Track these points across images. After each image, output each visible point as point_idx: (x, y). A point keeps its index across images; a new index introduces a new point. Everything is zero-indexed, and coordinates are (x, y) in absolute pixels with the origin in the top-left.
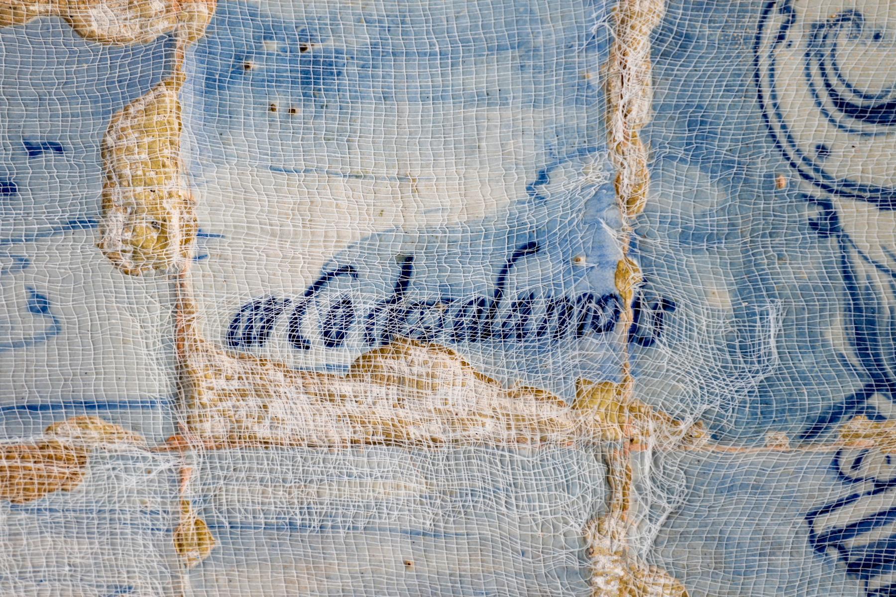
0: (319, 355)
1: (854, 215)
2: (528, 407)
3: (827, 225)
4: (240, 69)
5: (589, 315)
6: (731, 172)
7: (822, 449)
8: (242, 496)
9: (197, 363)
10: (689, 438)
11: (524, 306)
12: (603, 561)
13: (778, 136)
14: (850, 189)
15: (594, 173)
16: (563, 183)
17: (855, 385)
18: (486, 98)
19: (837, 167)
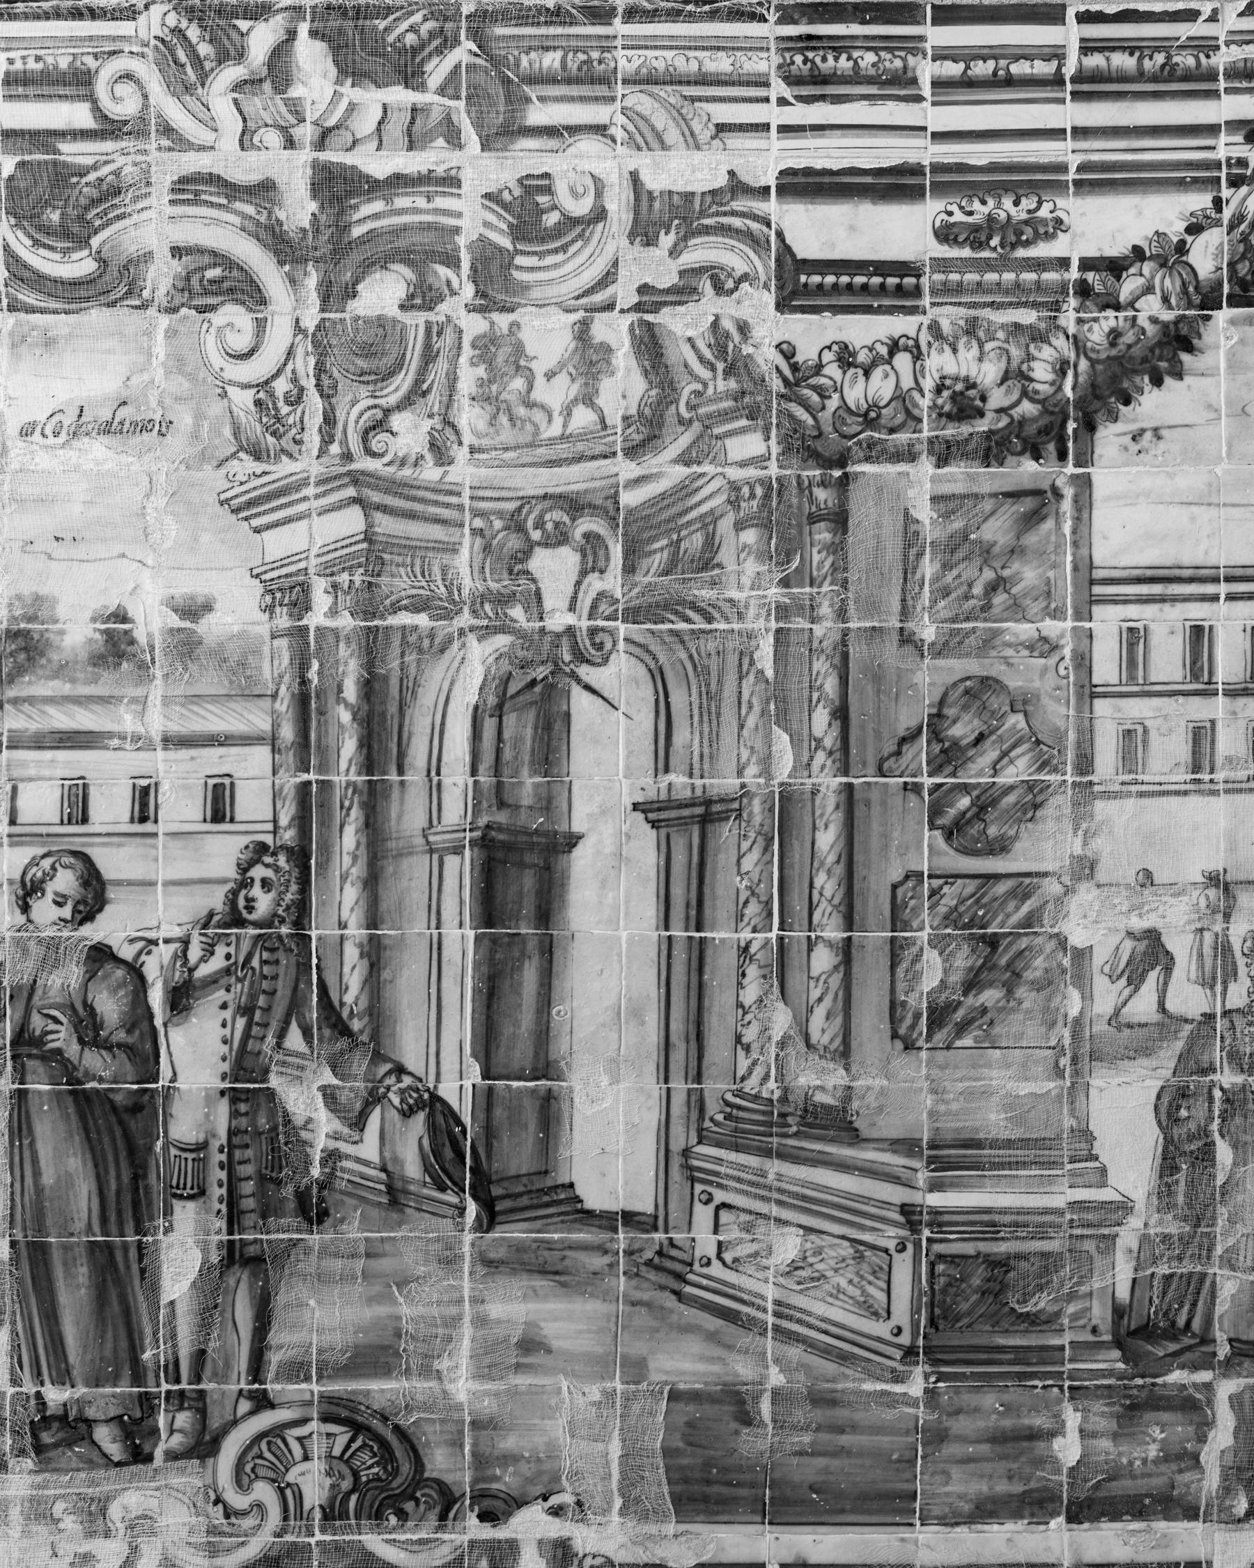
0: (51, 440)
1: (233, 391)
2: (125, 459)
3: (224, 395)
4: (23, 340)
5: (144, 427)
6: (192, 377)
7: (223, 471)
8: (25, 490)
9: (9, 443)
10: (177, 470)
11: (122, 423)
12: (149, 511)
13: (207, 365)
14: (231, 383)
15: (146, 377)
16: (135, 381)
17: (234, 449)
18: (109, 352)
19: (227, 375)
